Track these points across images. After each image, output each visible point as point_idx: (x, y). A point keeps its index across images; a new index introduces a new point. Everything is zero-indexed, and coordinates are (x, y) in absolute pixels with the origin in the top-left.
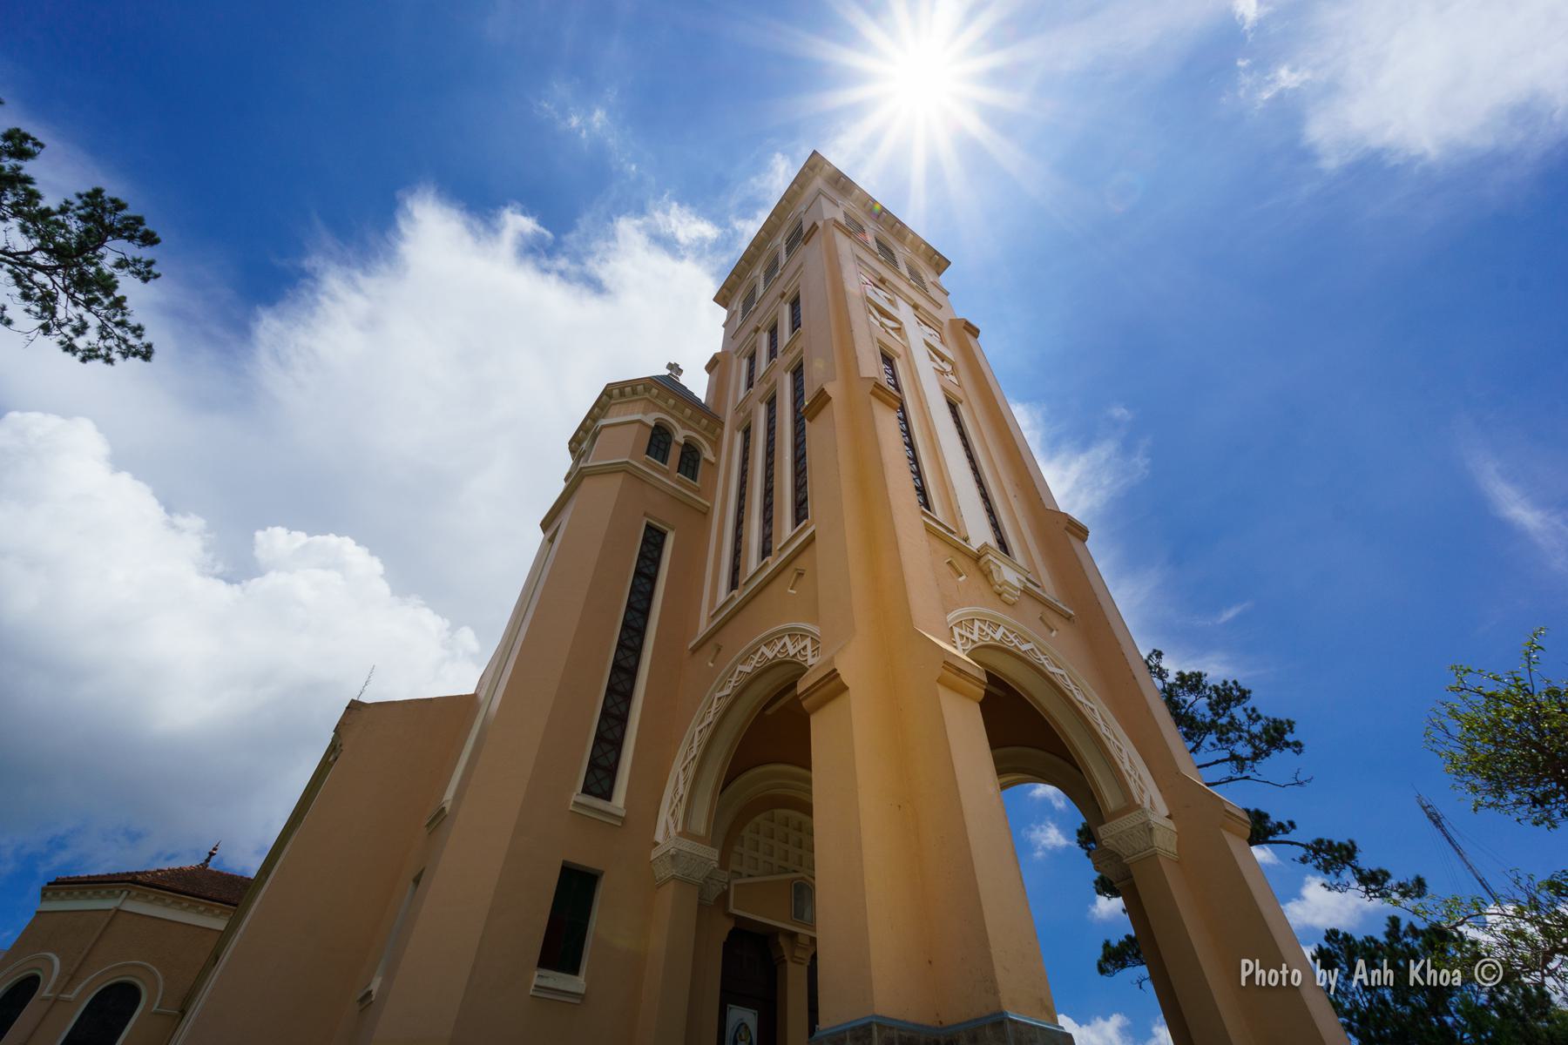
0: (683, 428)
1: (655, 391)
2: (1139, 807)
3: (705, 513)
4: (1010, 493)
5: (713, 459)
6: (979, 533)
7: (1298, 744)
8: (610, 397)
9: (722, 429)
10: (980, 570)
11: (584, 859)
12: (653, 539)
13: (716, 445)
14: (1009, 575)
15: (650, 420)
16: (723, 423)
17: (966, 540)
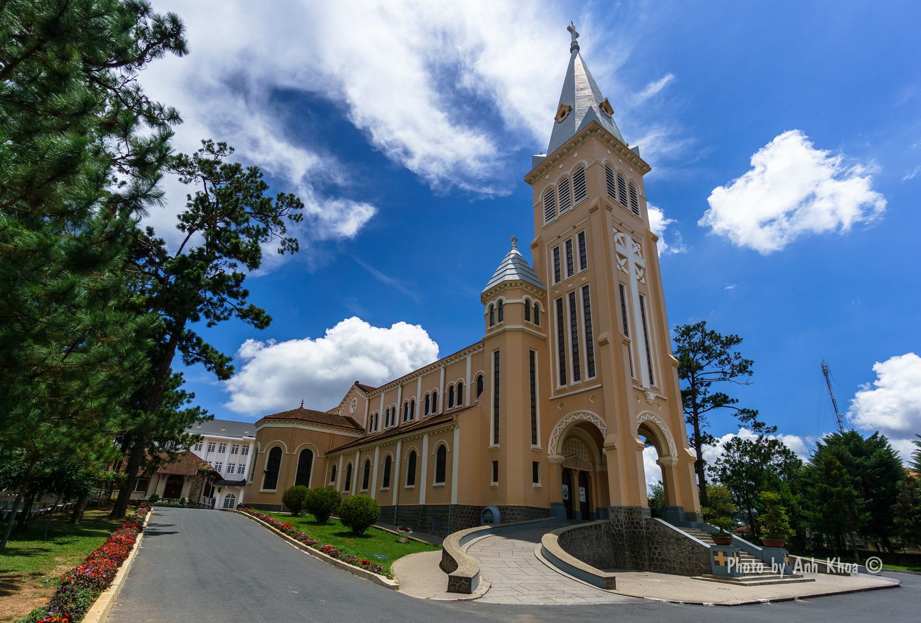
0: (533, 298)
1: (524, 285)
2: (671, 456)
3: (545, 340)
4: (656, 347)
5: (543, 310)
6: (646, 384)
7: (751, 372)
8: (505, 285)
9: (546, 294)
10: (644, 395)
11: (536, 461)
12: (532, 354)
13: (544, 301)
14: (652, 396)
15: (523, 301)
16: (546, 291)
17: (641, 387)
